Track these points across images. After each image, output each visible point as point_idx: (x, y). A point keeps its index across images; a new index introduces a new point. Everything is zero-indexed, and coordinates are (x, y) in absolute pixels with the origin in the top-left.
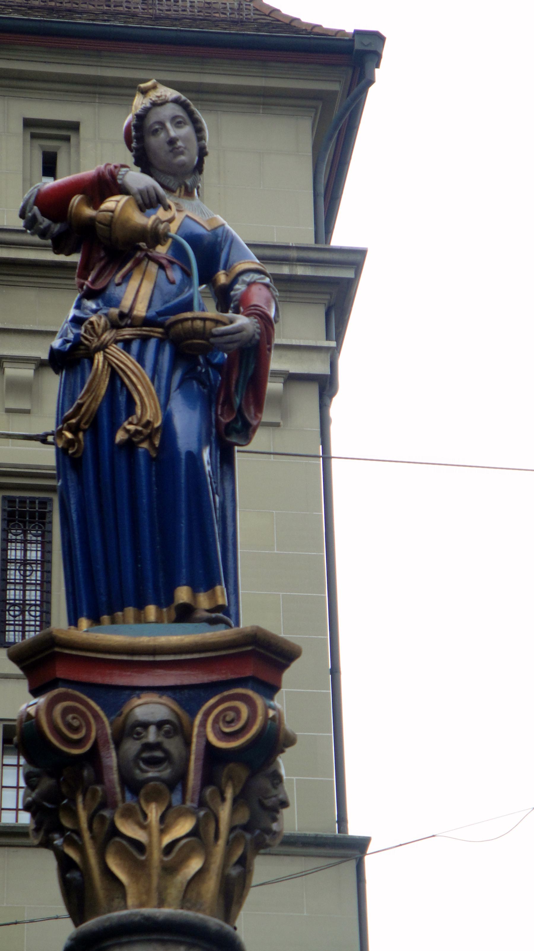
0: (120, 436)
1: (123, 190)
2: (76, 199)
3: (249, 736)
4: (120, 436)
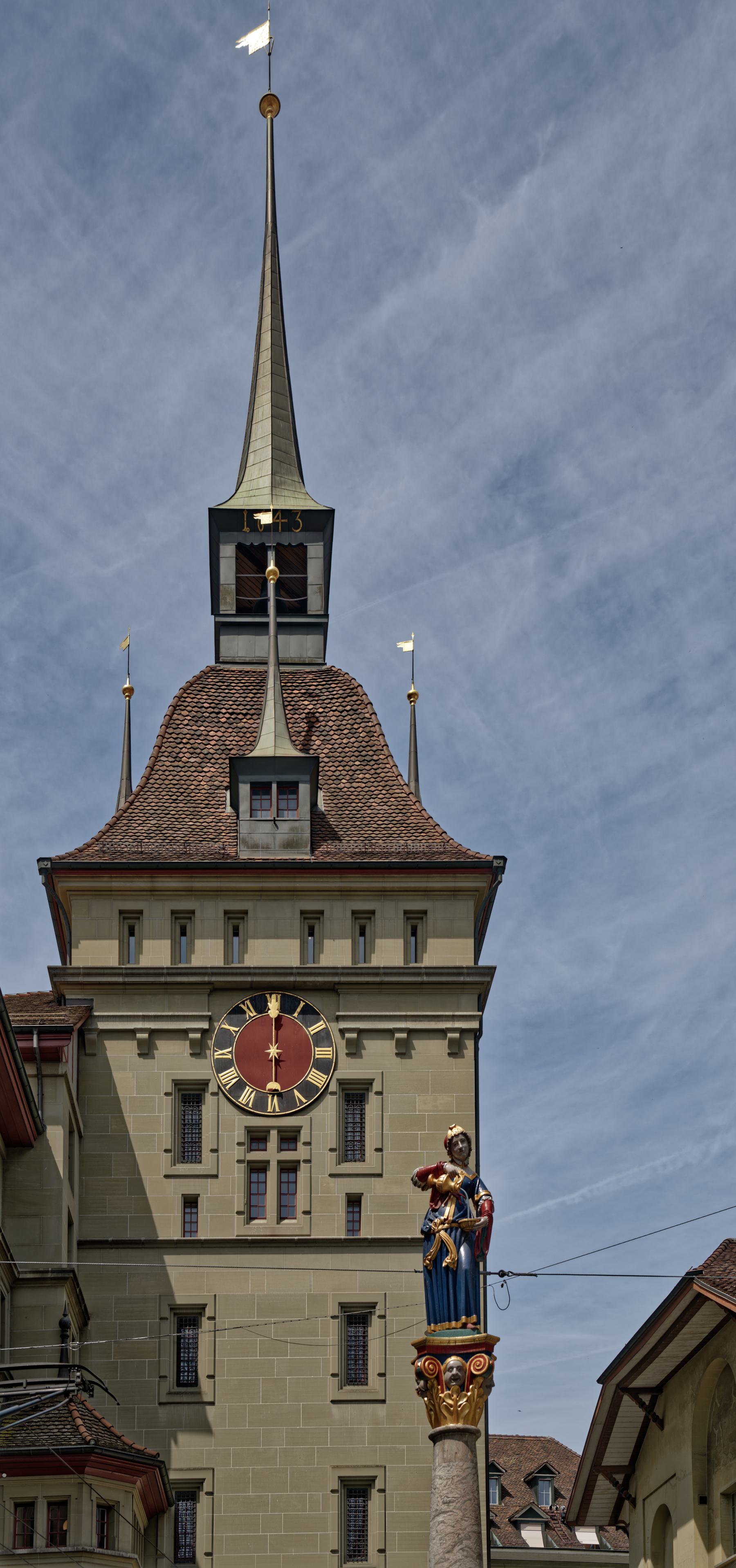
0: (444, 1264)
1: (445, 1173)
2: (430, 1176)
3: (484, 1370)
4: (444, 1264)
